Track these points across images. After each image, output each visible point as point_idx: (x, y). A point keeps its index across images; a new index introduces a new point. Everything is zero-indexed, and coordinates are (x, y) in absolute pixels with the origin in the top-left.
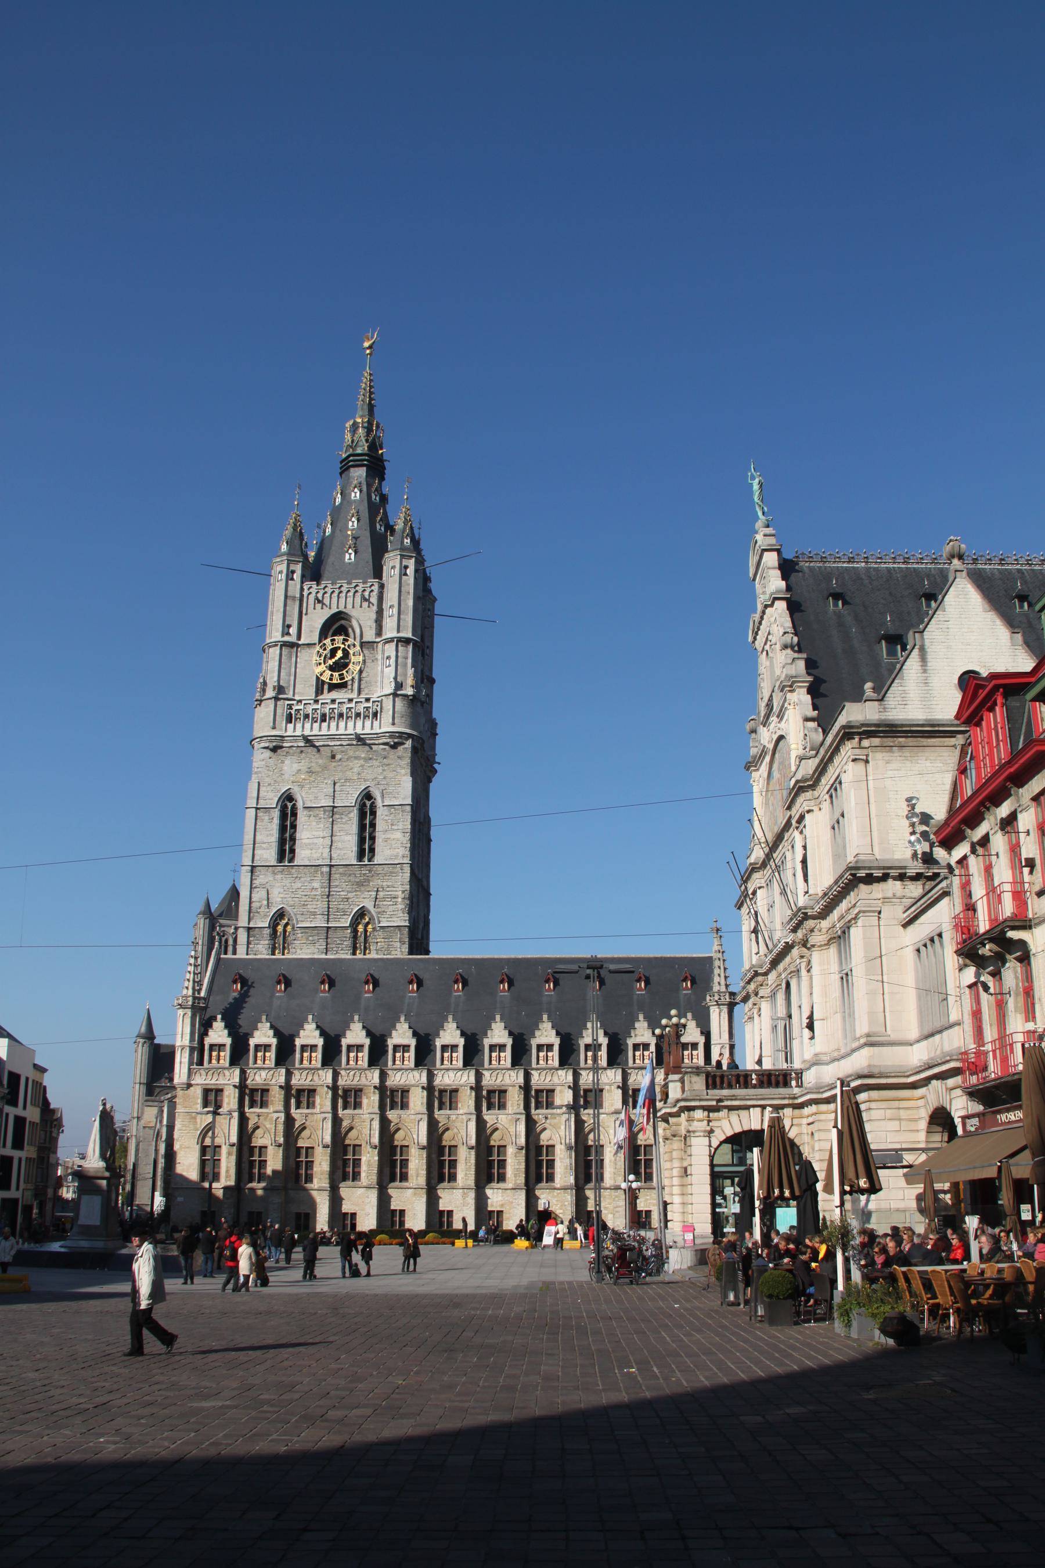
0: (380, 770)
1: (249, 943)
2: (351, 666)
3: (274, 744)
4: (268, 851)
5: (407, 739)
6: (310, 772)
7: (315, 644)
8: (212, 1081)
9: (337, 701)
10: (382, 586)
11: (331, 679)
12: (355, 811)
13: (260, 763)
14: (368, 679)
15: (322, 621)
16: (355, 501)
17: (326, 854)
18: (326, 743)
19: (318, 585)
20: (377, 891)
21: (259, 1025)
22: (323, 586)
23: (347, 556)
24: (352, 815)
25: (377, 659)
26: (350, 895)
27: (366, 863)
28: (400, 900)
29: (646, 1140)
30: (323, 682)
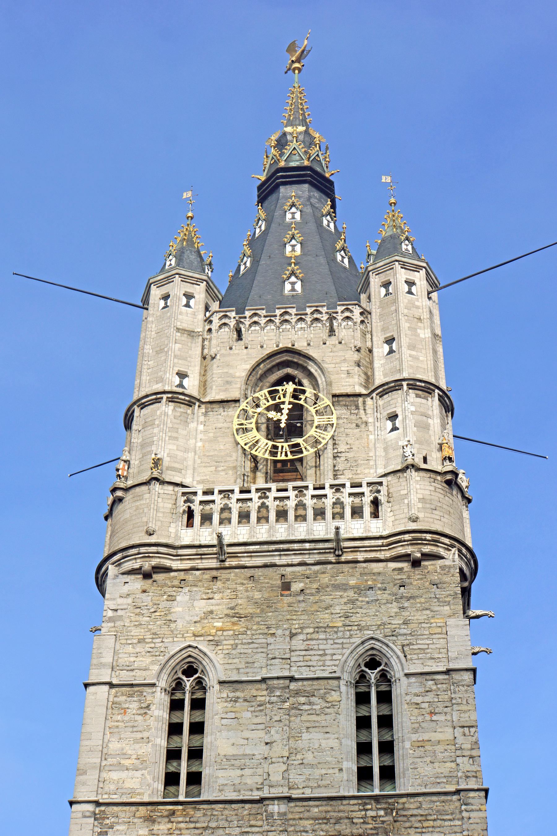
0: (394, 608)
2: (312, 432)
4: (138, 774)
5: (448, 548)
7: (237, 401)
11: (273, 453)
12: (343, 688)
13: (120, 601)
14: (349, 455)
15: (248, 366)
17: (276, 778)
19: (240, 311)
22: (248, 314)
23: (288, 287)
24: (334, 696)
25: (366, 423)
27: (377, 792)
30: (255, 459)
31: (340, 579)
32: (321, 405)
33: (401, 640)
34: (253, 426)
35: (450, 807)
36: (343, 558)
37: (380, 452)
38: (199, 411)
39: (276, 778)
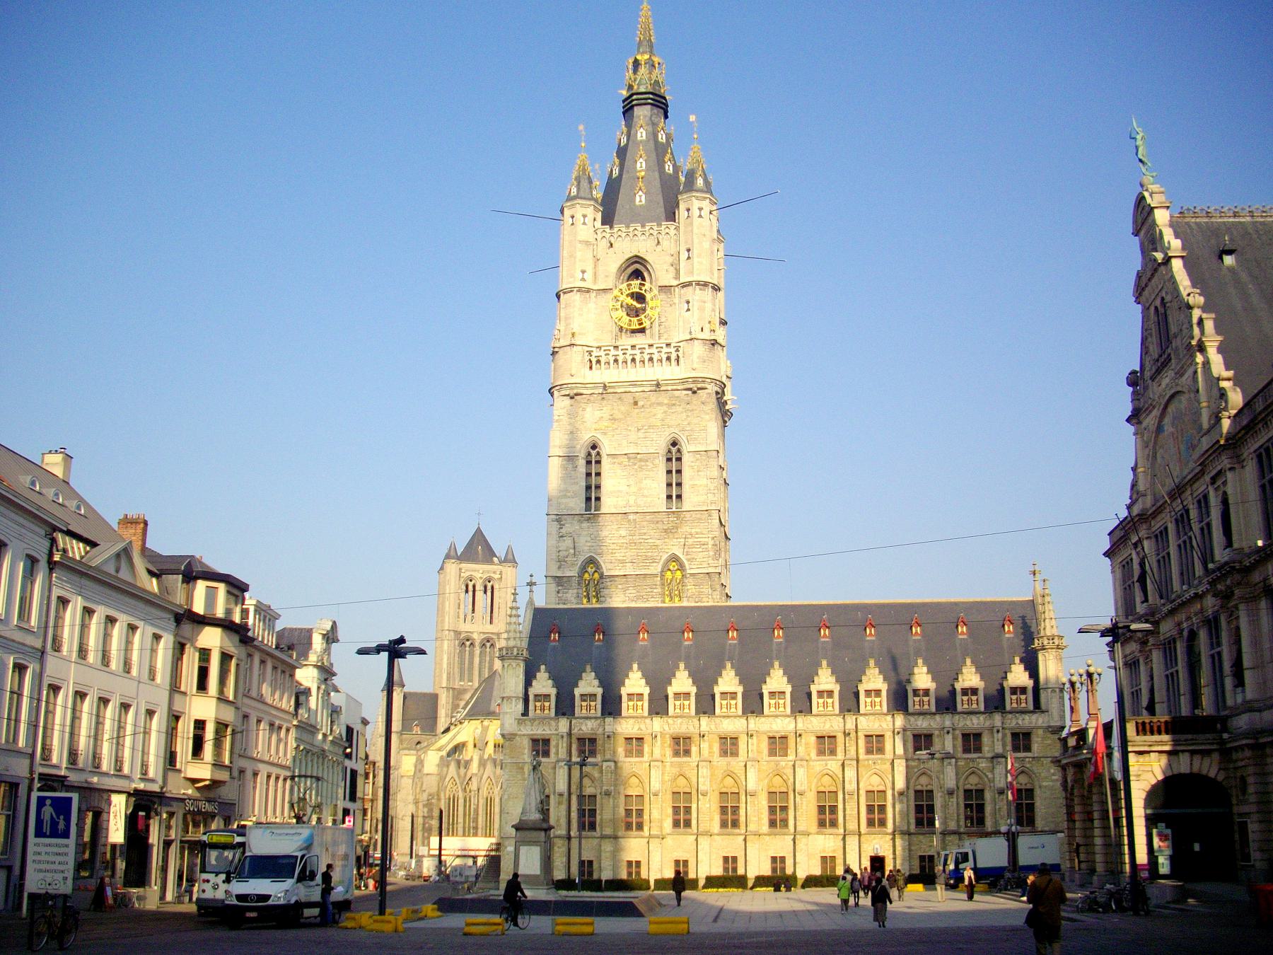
1: (558, 592)
3: (575, 391)
6: (613, 419)
8: (540, 731)
9: (638, 347)
10: (677, 228)
12: (661, 458)
13: (561, 411)
15: (618, 265)
16: (641, 141)
17: (632, 502)
18: (628, 390)
19: (611, 227)
20: (685, 538)
21: (584, 674)
24: (657, 461)
25: (675, 304)
26: (658, 542)
27: (674, 509)
28: (710, 546)
29: (976, 785)
31: (660, 400)
32: (652, 294)
33: (686, 433)
34: (619, 307)
35: (703, 517)
36: (662, 388)
37: (681, 324)
38: (593, 295)
39: (632, 502)
